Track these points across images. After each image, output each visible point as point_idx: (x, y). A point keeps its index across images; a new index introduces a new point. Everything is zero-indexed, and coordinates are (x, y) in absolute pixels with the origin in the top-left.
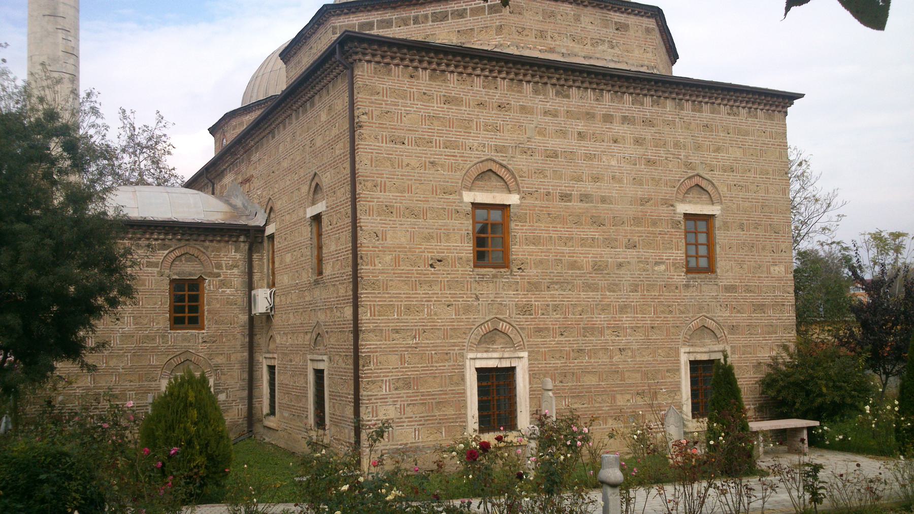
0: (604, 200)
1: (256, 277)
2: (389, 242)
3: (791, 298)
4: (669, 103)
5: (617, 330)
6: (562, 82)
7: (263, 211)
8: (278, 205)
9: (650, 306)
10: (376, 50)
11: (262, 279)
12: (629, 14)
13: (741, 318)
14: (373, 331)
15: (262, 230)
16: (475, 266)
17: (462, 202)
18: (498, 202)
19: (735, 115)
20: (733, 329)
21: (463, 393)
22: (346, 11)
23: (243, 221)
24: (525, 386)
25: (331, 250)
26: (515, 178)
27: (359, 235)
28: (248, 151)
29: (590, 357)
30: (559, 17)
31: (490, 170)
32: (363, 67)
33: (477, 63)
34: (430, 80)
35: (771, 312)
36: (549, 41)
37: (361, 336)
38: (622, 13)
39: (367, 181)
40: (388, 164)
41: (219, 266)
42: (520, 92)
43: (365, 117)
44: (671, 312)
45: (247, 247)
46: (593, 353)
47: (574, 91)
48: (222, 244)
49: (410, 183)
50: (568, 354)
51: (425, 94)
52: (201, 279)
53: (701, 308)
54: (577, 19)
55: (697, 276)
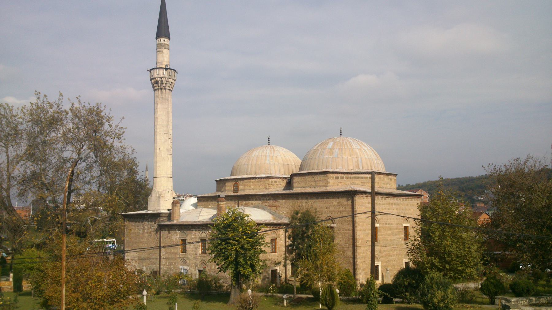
5: (394, 255)
46: (390, 261)
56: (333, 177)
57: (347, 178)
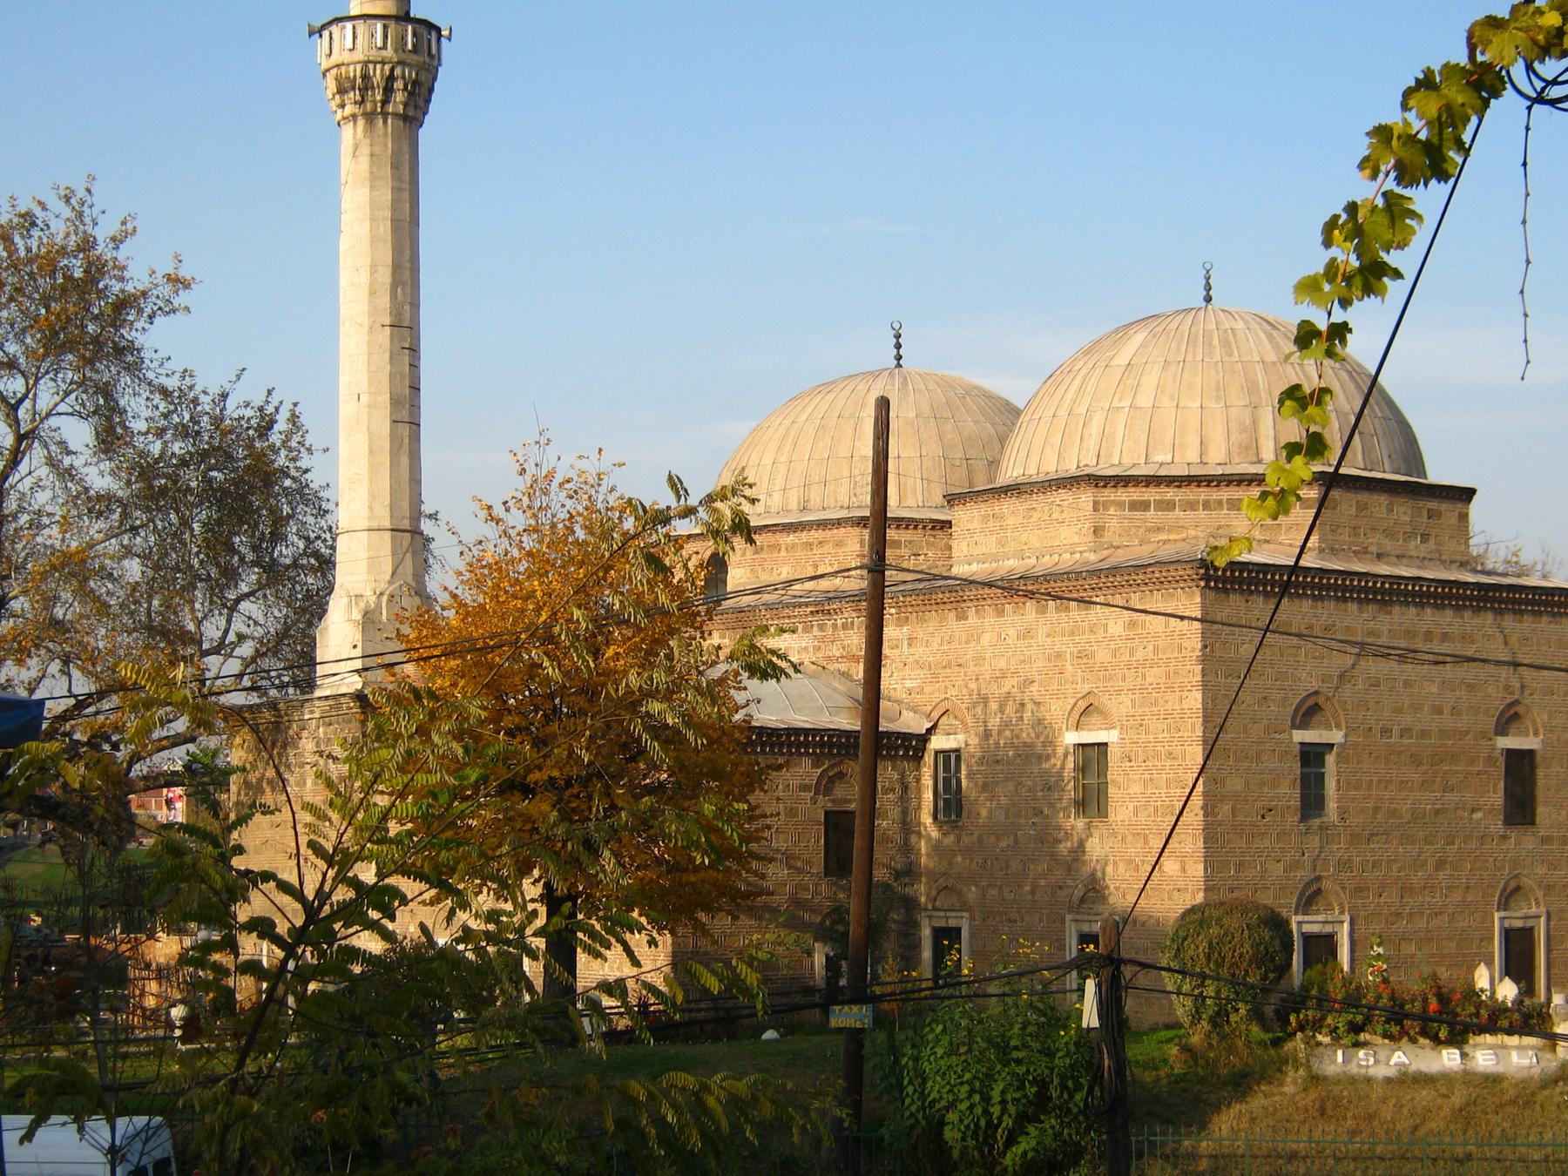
18: (1324, 741)
56: (1120, 505)
57: (1191, 506)
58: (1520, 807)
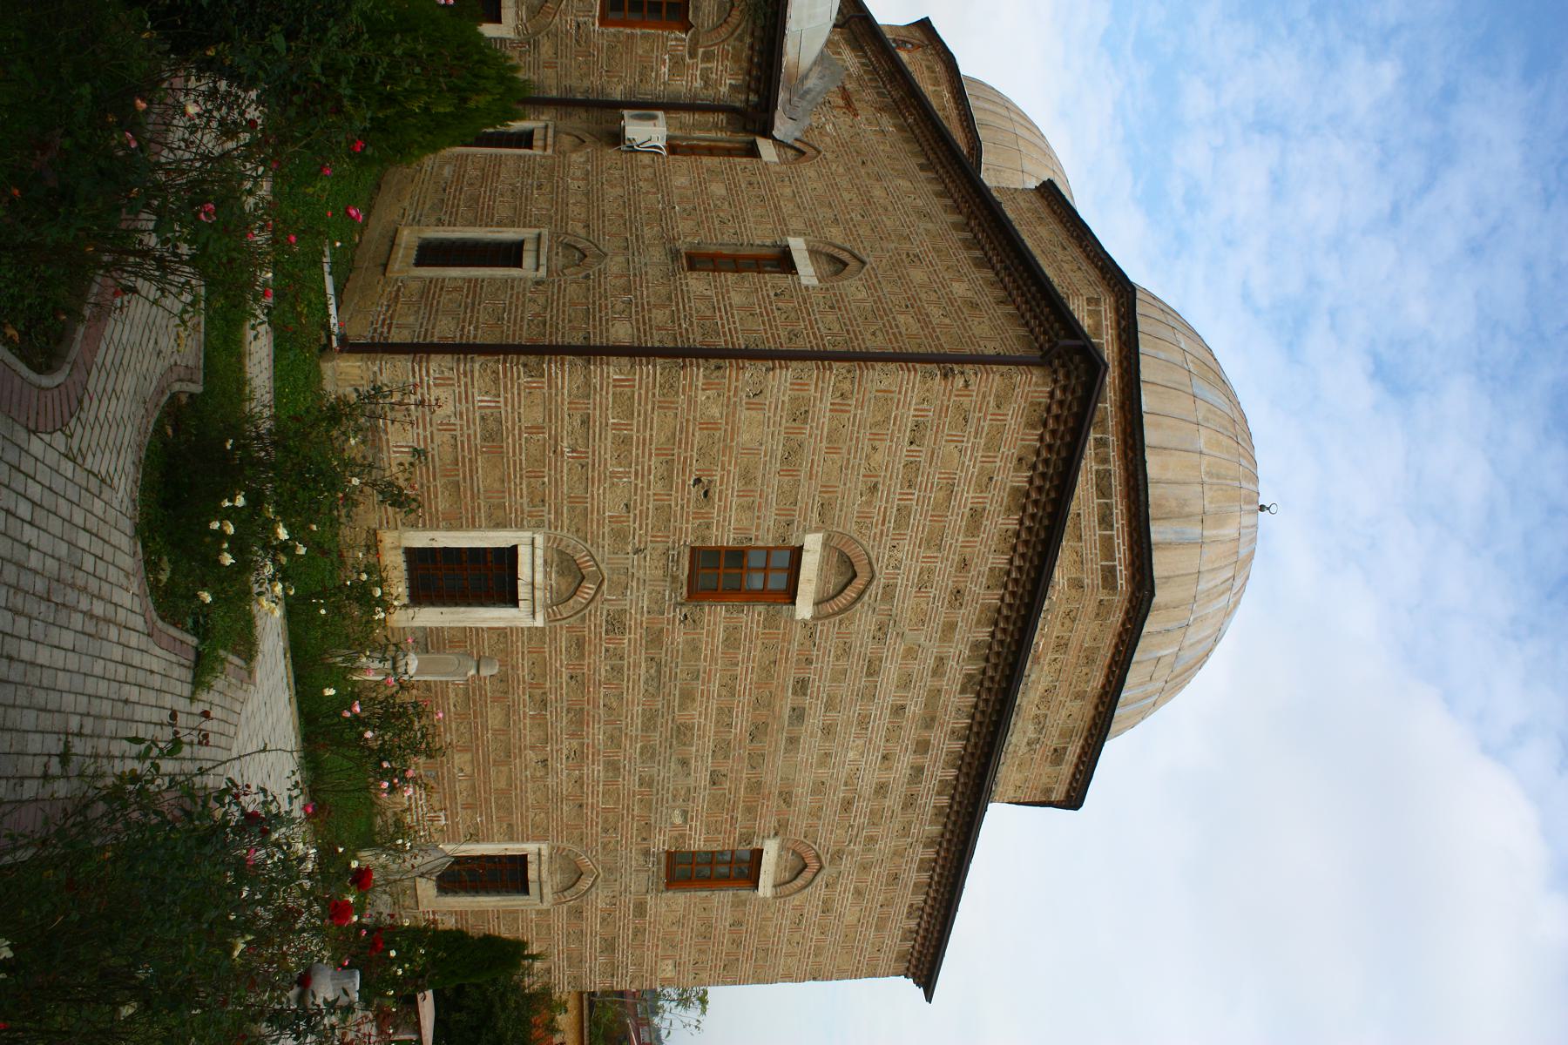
0: (793, 741)
1: (687, 118)
2: (744, 414)
3: (622, 985)
4: (937, 829)
5: (578, 757)
6: (987, 684)
7: (798, 134)
8: (808, 170)
9: (617, 802)
10: (1070, 408)
11: (682, 126)
12: (1077, 766)
13: (593, 923)
14: (587, 384)
15: (767, 132)
16: (693, 549)
17: (805, 531)
19: (910, 914)
20: (577, 913)
21: (473, 525)
22: (1123, 323)
23: (782, 96)
24: (485, 620)
25: (732, 294)
26: (837, 614)
27: (759, 363)
28: (895, 109)
29: (532, 717)
30: (1085, 670)
31: (855, 575)
32: (1045, 384)
33: (1031, 561)
34: (1012, 488)
35: (601, 960)
36: (1050, 656)
37: (579, 361)
38: (1080, 757)
39: (852, 383)
40: (879, 418)
41: (708, 57)
42: (978, 622)
43: (961, 383)
44: (606, 831)
45: (738, 104)
46: (540, 722)
47: (970, 699)
48: (745, 65)
49: (844, 451)
50: (539, 686)
51: (991, 479)
52: (686, 27)
53: (610, 871)
54: (1080, 696)
55: (663, 866)
58: (685, 871)
